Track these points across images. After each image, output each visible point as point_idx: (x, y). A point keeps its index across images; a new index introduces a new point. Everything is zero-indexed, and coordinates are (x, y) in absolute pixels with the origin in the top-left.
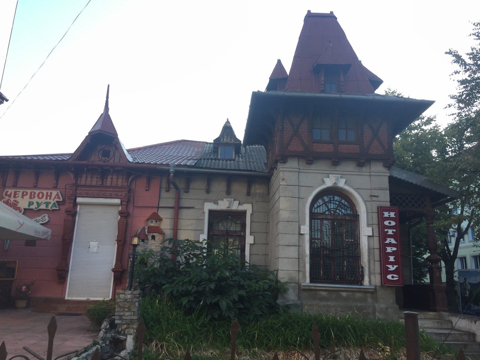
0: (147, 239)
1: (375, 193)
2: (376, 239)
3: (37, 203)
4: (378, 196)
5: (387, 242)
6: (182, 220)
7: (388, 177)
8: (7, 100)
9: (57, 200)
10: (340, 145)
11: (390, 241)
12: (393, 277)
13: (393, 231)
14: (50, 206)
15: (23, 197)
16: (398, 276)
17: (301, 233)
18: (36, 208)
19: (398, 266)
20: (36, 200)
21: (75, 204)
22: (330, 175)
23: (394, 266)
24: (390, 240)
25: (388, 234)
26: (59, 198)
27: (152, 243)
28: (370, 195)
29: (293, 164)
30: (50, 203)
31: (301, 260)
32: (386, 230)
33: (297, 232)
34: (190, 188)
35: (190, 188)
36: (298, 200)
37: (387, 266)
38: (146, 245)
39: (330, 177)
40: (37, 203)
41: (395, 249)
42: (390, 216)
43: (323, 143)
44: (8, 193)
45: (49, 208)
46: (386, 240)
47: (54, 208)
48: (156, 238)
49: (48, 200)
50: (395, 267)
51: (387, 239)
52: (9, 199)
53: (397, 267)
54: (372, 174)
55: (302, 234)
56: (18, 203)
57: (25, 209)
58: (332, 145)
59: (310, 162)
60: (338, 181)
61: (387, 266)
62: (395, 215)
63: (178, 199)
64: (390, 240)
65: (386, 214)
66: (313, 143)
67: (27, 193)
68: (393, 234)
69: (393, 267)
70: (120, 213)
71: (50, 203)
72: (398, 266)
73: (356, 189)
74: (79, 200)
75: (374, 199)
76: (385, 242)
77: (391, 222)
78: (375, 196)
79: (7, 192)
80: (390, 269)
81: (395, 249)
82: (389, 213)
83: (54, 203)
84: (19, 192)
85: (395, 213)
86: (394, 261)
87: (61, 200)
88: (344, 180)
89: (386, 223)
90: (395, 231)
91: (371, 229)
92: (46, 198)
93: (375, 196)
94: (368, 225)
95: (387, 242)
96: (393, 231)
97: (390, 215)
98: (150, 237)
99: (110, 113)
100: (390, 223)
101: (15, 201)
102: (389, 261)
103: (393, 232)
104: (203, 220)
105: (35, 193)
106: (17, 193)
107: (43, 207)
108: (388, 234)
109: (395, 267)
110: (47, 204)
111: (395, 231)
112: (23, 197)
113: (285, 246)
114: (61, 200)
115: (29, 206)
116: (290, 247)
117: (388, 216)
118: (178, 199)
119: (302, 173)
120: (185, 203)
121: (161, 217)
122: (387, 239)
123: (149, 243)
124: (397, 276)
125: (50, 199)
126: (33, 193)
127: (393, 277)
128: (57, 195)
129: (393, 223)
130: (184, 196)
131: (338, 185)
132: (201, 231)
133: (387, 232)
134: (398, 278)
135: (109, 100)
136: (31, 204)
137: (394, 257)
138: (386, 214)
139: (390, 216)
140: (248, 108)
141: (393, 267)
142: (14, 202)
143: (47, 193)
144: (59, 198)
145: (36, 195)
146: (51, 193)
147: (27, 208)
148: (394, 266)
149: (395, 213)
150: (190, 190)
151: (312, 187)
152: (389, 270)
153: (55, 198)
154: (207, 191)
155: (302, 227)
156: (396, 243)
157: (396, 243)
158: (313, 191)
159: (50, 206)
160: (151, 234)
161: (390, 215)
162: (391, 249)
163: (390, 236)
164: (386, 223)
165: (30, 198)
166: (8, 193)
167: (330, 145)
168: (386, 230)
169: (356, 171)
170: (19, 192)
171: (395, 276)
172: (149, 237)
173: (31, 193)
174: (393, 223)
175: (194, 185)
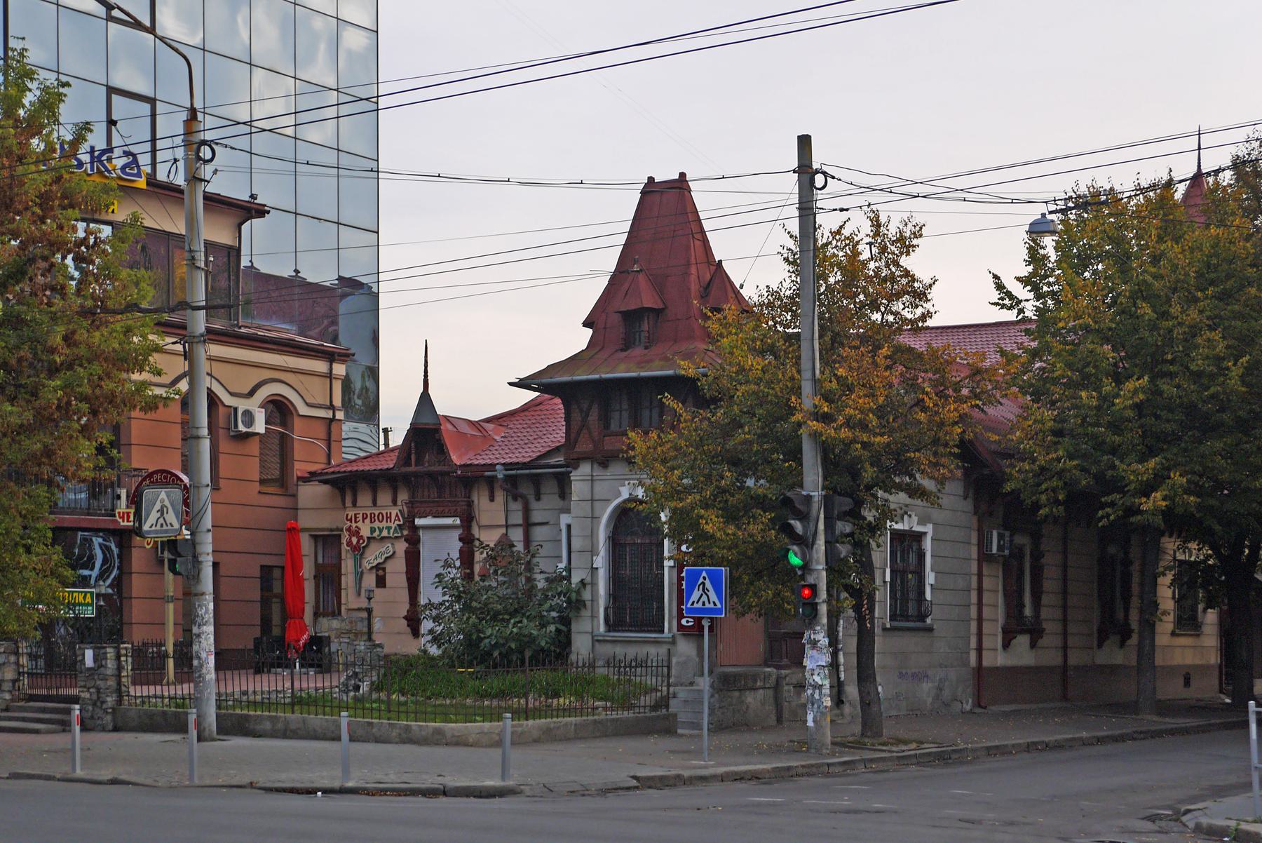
9: (397, 522)
14: (392, 531)
15: (363, 522)
17: (594, 566)
18: (378, 536)
20: (376, 524)
21: (415, 529)
26: (399, 520)
29: (585, 469)
31: (595, 603)
36: (592, 522)
44: (349, 517)
47: (396, 535)
49: (389, 524)
55: (597, 568)
57: (368, 538)
59: (604, 464)
63: (527, 511)
70: (460, 539)
71: (391, 527)
74: (419, 522)
79: (347, 515)
87: (401, 523)
101: (356, 527)
104: (560, 540)
107: (385, 533)
110: (389, 528)
112: (363, 522)
114: (401, 523)
118: (527, 511)
120: (537, 517)
127: (688, 622)
128: (397, 515)
130: (534, 505)
144: (399, 520)
147: (369, 535)
150: (542, 496)
151: (608, 501)
154: (560, 496)
159: (392, 531)
165: (371, 522)
166: (349, 517)
173: (371, 514)
175: (543, 490)
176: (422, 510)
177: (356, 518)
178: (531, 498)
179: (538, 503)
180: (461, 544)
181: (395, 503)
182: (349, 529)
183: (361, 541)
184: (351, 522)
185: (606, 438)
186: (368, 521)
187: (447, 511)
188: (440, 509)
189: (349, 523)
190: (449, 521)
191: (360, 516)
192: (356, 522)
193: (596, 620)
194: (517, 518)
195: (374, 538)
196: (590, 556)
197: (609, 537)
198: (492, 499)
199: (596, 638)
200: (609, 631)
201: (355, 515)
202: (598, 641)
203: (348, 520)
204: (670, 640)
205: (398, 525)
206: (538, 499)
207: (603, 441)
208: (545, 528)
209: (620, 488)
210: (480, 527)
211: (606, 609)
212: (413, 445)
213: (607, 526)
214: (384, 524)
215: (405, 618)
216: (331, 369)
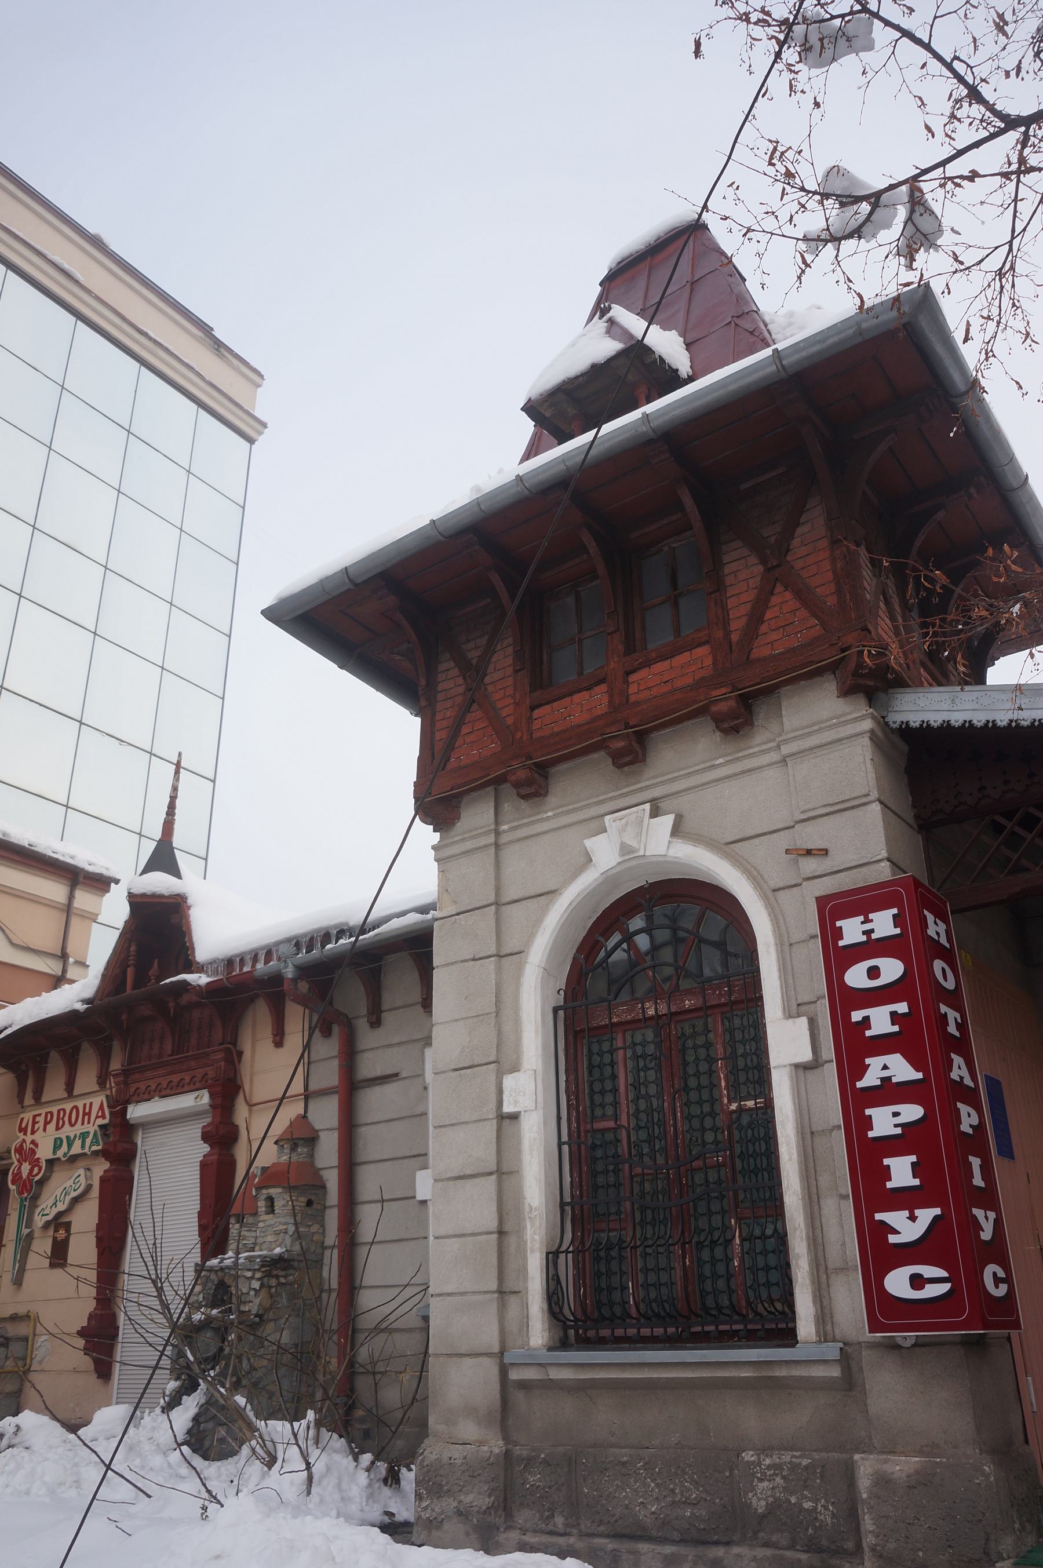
0: (255, 1214)
1: (812, 836)
2: (830, 1072)
3: (68, 1137)
4: (825, 852)
5: (871, 1079)
6: (369, 1127)
7: (866, 741)
8: (117, 882)
9: (100, 1121)
10: (633, 678)
11: (886, 1074)
12: (917, 1281)
13: (894, 1015)
15: (45, 1130)
16: (944, 1274)
17: (508, 1108)
18: (65, 1155)
19: (937, 1211)
22: (607, 819)
23: (917, 1212)
24: (885, 1067)
25: (868, 1033)
27: (267, 1223)
28: (787, 851)
30: (88, 1133)
31: (512, 1241)
32: (857, 1016)
33: (492, 1115)
34: (384, 1008)
35: (385, 1006)
36: (499, 970)
37: (878, 1216)
38: (247, 1234)
39: (607, 825)
40: (68, 1137)
41: (912, 1112)
42: (874, 936)
43: (571, 694)
44: (23, 1126)
45: (86, 1150)
46: (861, 1070)
47: (94, 1148)
48: (278, 1204)
50: (926, 1216)
51: (868, 1061)
52: (24, 1141)
53: (936, 1218)
54: (785, 750)
55: (515, 1117)
56: (36, 1145)
58: (603, 687)
60: (639, 834)
61: (878, 1216)
62: (897, 920)
63: (349, 1055)
64: (885, 1067)
65: (852, 931)
66: (533, 708)
67: (51, 1113)
68: (896, 1028)
69: (913, 1218)
70: (206, 1137)
72: (937, 1211)
73: (727, 848)
74: (136, 1112)
75: (810, 866)
76: (859, 1085)
77: (882, 963)
78: (809, 852)
79: (22, 1119)
80: (898, 1233)
81: (912, 1112)
82: (867, 921)
83: (95, 1132)
84: (39, 1115)
85: (895, 911)
86: (917, 1182)
88: (667, 821)
89: (856, 977)
90: (902, 1008)
91: (803, 1022)
92: (83, 1124)
93: (809, 852)
94: (792, 1010)
95: (871, 1079)
96: (894, 1015)
97: (872, 931)
98: (262, 1204)
99: (177, 841)
100: (874, 973)
101: (33, 1142)
102: (889, 1185)
103: (895, 1017)
105: (64, 1110)
106: (38, 1119)
107: (76, 1149)
108: (868, 1033)
109: (926, 1216)
110: (84, 1136)
111: (902, 1008)
112: (45, 1130)
113: (451, 1183)
114: (106, 1121)
115: (54, 1153)
116: (469, 1184)
117: (864, 938)
119: (517, 846)
120: (369, 1065)
121: (317, 1127)
122: (868, 1061)
123: (261, 1225)
124: (941, 1273)
125: (89, 1123)
126: (62, 1113)
127: (917, 1281)
128: (101, 1107)
129: (891, 969)
130: (367, 1038)
131: (641, 853)
132: (422, 1158)
133: (866, 1022)
134: (946, 1287)
135: (178, 801)
136: (57, 1144)
137: (913, 1158)
138: (852, 931)
139: (874, 936)
140: (345, 674)
141: (913, 1218)
142: (31, 1146)
143: (85, 1105)
144: (103, 1117)
145: (66, 1119)
146: (91, 1104)
147: (51, 1156)
148: (917, 1212)
149: (895, 911)
151: (552, 893)
152: (893, 1239)
153: (97, 1117)
155: (508, 1081)
156: (919, 1076)
157: (919, 1076)
158: (544, 911)
159: (88, 1141)
160: (264, 1191)
161: (872, 931)
162: (896, 1114)
163: (883, 1045)
164: (856, 977)
165: (58, 1128)
167: (597, 689)
168: (857, 1016)
169: (721, 761)
170: (39, 1115)
171: (929, 1271)
172: (259, 1204)
173: (59, 1111)
174: (891, 969)
175: (388, 999)
176: (142, 1086)
177: (34, 1122)
178: (362, 1025)
179: (380, 1031)
180: (206, 1148)
181: (102, 1081)
182: (19, 1150)
183: (36, 1170)
184: (25, 1134)
185: (536, 713)
186: (51, 1127)
187: (187, 1079)
188: (176, 1078)
189: (21, 1136)
190: (186, 1102)
191: (41, 1120)
192: (33, 1132)
193: (513, 1301)
194: (328, 1075)
195: (59, 1159)
196: (493, 1077)
197: (556, 1010)
198: (279, 1043)
199: (514, 1375)
200: (563, 1344)
201: (35, 1117)
202: (524, 1385)
203: (21, 1130)
204: (835, 1372)
205: (101, 1127)
206: (376, 1022)
207: (530, 720)
208: (389, 1090)
209: (589, 843)
210: (251, 1105)
211: (552, 1257)
212: (133, 948)
213: (547, 972)
214: (79, 1129)
215: (82, 1333)
216: (71, 897)
